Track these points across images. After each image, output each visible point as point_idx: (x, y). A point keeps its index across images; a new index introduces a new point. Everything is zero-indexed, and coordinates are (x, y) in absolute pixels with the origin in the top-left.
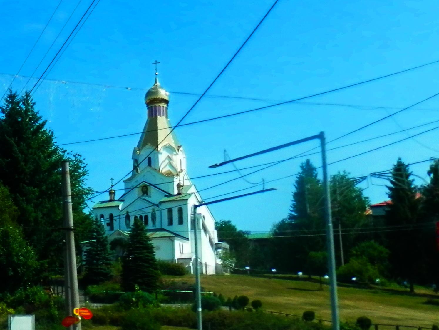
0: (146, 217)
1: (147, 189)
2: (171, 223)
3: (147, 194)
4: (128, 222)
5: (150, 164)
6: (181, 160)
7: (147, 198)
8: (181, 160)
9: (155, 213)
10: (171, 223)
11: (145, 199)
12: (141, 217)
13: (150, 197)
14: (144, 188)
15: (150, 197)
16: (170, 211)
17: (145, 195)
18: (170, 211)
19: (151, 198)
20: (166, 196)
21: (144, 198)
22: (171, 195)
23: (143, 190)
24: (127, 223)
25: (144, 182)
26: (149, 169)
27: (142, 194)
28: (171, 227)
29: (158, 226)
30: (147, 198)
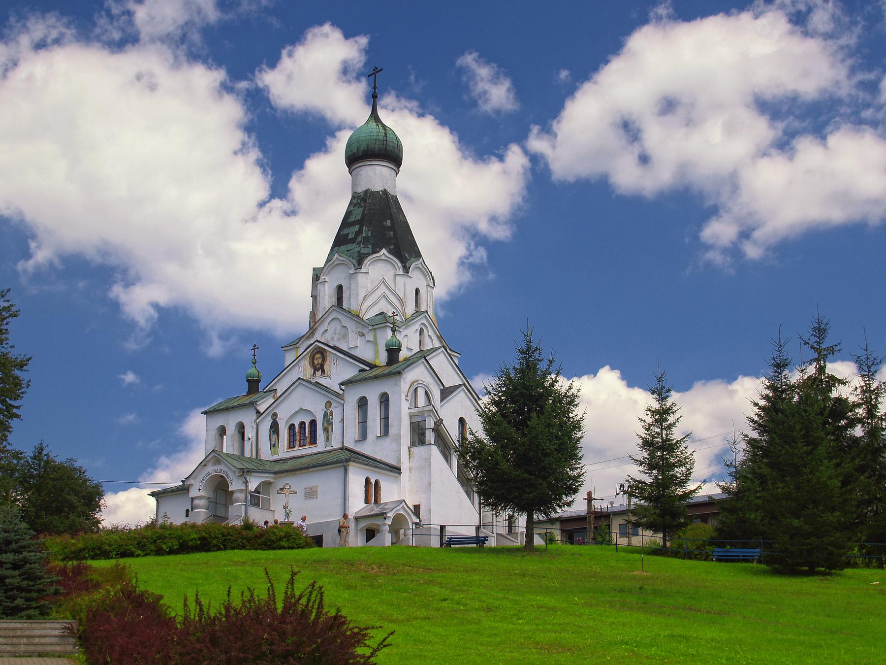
0: (313, 423)
1: (324, 359)
3: (323, 371)
4: (274, 437)
7: (323, 381)
12: (302, 424)
13: (329, 376)
14: (318, 355)
15: (329, 376)
16: (363, 403)
17: (319, 373)
18: (363, 403)
19: (331, 379)
22: (372, 366)
23: (316, 362)
24: (273, 443)
25: (317, 343)
27: (313, 370)
29: (336, 444)
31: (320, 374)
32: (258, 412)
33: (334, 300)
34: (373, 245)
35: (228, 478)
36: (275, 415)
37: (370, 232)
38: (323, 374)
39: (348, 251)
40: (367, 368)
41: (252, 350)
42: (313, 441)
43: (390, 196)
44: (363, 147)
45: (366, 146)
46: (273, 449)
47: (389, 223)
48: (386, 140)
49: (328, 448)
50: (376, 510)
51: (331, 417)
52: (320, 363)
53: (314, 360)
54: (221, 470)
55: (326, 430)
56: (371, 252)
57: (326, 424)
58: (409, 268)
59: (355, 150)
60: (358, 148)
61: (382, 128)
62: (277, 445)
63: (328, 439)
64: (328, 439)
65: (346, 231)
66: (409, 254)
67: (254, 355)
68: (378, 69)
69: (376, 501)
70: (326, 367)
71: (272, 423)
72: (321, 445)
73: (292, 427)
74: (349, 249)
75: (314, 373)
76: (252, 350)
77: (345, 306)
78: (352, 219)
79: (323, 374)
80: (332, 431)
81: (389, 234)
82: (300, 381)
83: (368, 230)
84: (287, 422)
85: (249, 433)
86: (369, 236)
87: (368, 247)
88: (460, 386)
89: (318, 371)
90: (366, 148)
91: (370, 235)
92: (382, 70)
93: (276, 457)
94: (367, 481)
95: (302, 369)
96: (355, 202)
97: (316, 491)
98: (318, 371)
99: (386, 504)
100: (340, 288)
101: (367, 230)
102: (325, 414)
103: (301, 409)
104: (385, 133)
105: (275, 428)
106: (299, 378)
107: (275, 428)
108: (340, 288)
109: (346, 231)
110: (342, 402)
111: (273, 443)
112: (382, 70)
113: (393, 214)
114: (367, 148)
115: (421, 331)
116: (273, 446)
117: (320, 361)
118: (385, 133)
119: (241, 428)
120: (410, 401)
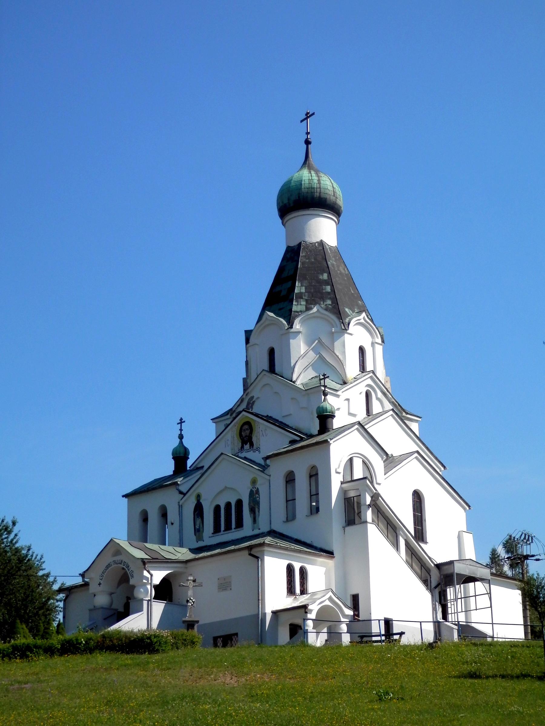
0: (239, 503)
2: (291, 517)
3: (252, 445)
5: (272, 369)
6: (362, 350)
7: (251, 455)
8: (362, 350)
9: (257, 491)
10: (291, 517)
11: (245, 459)
12: (228, 505)
13: (258, 449)
14: (246, 427)
16: (290, 479)
17: (247, 447)
18: (290, 479)
19: (260, 452)
20: (293, 442)
21: (243, 455)
25: (244, 413)
26: (269, 378)
27: (240, 444)
28: (290, 524)
30: (251, 455)
31: (249, 448)
32: (181, 493)
33: (265, 365)
34: (307, 301)
35: (129, 570)
36: (198, 497)
37: (304, 288)
38: (251, 447)
39: (280, 309)
40: (298, 439)
41: (178, 424)
42: (240, 524)
43: (327, 247)
44: (293, 198)
45: (297, 196)
46: (197, 534)
47: (325, 276)
48: (320, 188)
49: (256, 532)
50: (301, 600)
51: (257, 495)
52: (248, 434)
53: (242, 432)
54: (122, 561)
55: (253, 511)
56: (304, 309)
57: (252, 504)
58: (349, 324)
59: (286, 201)
60: (289, 199)
61: (315, 175)
62: (201, 530)
63: (255, 521)
64: (255, 521)
65: (278, 289)
66: (350, 309)
67: (181, 430)
68: (310, 113)
69: (303, 592)
70: (254, 439)
71: (196, 504)
72: (247, 530)
73: (217, 509)
74: (282, 307)
75: (242, 447)
76: (178, 424)
77: (277, 369)
78: (285, 274)
79: (251, 447)
80: (259, 512)
81: (325, 289)
82: (223, 456)
83: (302, 286)
84: (212, 502)
85: (172, 515)
86: (302, 293)
87: (301, 305)
88: (412, 453)
89: (246, 445)
90: (297, 198)
91: (303, 290)
92: (313, 114)
93: (201, 544)
94: (290, 569)
95: (229, 443)
96: (289, 257)
97: (230, 582)
98: (246, 445)
99: (314, 594)
100: (272, 352)
101: (300, 285)
102: (251, 491)
103: (226, 488)
104: (319, 180)
105: (199, 510)
106: (222, 454)
107: (199, 510)
108: (272, 352)
109: (278, 289)
110: (268, 477)
111: (197, 527)
112: (313, 114)
113: (330, 266)
114: (299, 197)
115: (368, 396)
116: (198, 531)
117: (248, 432)
118: (319, 180)
119: (164, 514)
120: (342, 474)
